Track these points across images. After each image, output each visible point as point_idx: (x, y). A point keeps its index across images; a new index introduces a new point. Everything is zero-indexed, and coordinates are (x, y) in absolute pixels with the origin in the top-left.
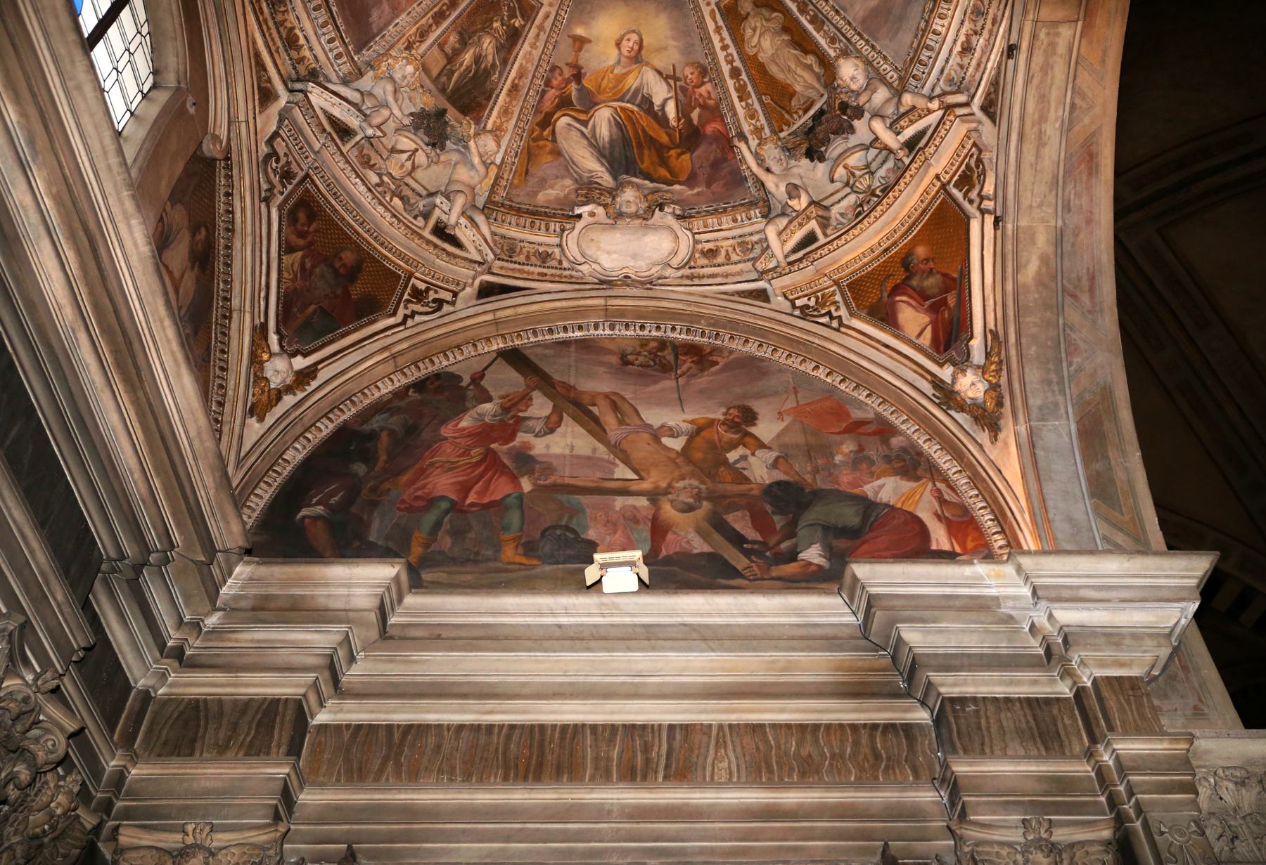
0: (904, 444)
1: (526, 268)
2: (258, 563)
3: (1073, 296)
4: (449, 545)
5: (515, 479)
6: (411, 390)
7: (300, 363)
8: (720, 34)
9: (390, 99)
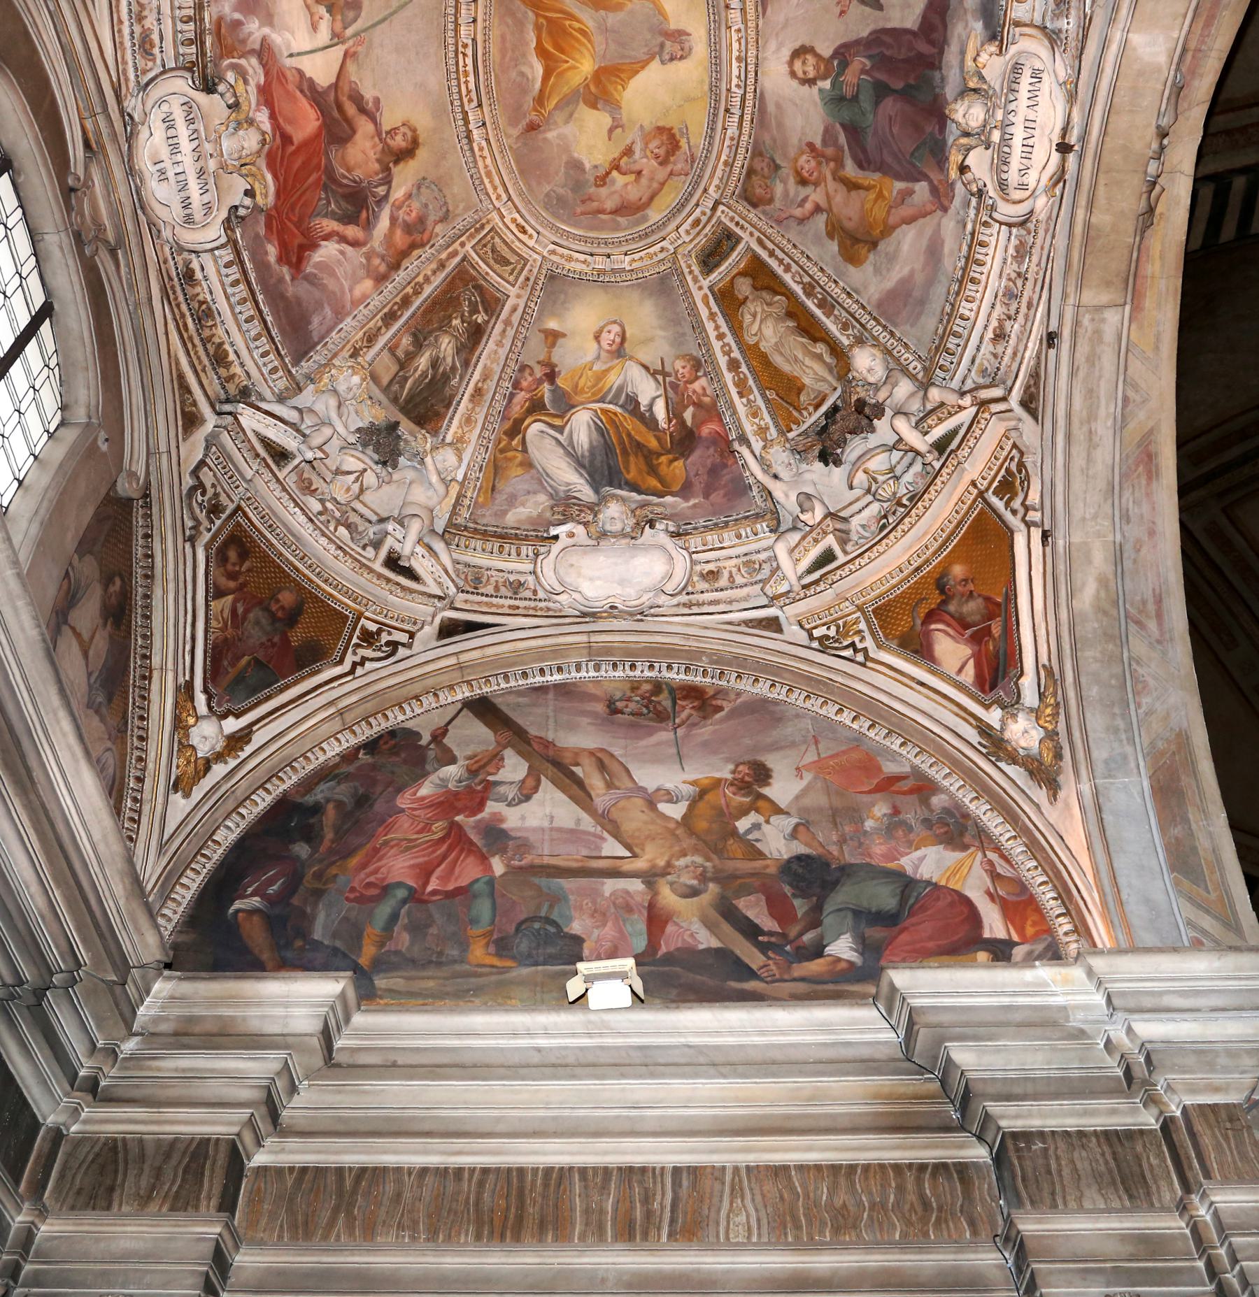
0: (946, 805)
1: (494, 600)
2: (180, 979)
3: (1138, 623)
4: (407, 943)
5: (484, 859)
6: (362, 752)
7: (232, 725)
8: (715, 321)
9: (333, 415)
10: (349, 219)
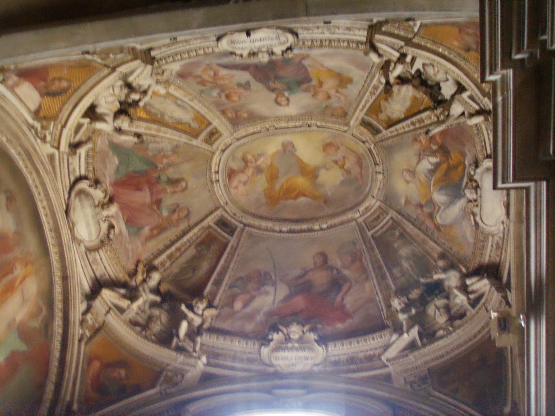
10: (340, 287)
